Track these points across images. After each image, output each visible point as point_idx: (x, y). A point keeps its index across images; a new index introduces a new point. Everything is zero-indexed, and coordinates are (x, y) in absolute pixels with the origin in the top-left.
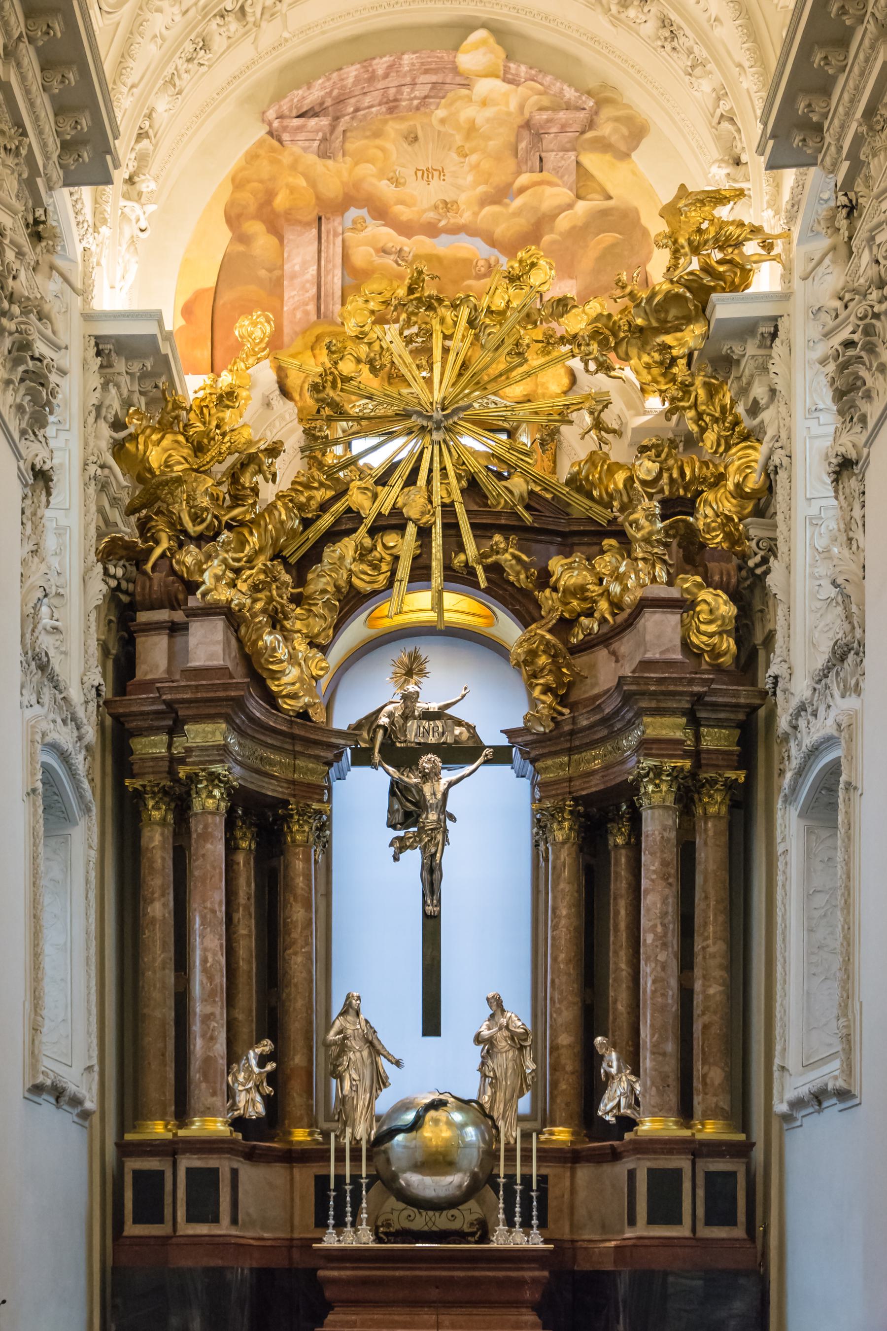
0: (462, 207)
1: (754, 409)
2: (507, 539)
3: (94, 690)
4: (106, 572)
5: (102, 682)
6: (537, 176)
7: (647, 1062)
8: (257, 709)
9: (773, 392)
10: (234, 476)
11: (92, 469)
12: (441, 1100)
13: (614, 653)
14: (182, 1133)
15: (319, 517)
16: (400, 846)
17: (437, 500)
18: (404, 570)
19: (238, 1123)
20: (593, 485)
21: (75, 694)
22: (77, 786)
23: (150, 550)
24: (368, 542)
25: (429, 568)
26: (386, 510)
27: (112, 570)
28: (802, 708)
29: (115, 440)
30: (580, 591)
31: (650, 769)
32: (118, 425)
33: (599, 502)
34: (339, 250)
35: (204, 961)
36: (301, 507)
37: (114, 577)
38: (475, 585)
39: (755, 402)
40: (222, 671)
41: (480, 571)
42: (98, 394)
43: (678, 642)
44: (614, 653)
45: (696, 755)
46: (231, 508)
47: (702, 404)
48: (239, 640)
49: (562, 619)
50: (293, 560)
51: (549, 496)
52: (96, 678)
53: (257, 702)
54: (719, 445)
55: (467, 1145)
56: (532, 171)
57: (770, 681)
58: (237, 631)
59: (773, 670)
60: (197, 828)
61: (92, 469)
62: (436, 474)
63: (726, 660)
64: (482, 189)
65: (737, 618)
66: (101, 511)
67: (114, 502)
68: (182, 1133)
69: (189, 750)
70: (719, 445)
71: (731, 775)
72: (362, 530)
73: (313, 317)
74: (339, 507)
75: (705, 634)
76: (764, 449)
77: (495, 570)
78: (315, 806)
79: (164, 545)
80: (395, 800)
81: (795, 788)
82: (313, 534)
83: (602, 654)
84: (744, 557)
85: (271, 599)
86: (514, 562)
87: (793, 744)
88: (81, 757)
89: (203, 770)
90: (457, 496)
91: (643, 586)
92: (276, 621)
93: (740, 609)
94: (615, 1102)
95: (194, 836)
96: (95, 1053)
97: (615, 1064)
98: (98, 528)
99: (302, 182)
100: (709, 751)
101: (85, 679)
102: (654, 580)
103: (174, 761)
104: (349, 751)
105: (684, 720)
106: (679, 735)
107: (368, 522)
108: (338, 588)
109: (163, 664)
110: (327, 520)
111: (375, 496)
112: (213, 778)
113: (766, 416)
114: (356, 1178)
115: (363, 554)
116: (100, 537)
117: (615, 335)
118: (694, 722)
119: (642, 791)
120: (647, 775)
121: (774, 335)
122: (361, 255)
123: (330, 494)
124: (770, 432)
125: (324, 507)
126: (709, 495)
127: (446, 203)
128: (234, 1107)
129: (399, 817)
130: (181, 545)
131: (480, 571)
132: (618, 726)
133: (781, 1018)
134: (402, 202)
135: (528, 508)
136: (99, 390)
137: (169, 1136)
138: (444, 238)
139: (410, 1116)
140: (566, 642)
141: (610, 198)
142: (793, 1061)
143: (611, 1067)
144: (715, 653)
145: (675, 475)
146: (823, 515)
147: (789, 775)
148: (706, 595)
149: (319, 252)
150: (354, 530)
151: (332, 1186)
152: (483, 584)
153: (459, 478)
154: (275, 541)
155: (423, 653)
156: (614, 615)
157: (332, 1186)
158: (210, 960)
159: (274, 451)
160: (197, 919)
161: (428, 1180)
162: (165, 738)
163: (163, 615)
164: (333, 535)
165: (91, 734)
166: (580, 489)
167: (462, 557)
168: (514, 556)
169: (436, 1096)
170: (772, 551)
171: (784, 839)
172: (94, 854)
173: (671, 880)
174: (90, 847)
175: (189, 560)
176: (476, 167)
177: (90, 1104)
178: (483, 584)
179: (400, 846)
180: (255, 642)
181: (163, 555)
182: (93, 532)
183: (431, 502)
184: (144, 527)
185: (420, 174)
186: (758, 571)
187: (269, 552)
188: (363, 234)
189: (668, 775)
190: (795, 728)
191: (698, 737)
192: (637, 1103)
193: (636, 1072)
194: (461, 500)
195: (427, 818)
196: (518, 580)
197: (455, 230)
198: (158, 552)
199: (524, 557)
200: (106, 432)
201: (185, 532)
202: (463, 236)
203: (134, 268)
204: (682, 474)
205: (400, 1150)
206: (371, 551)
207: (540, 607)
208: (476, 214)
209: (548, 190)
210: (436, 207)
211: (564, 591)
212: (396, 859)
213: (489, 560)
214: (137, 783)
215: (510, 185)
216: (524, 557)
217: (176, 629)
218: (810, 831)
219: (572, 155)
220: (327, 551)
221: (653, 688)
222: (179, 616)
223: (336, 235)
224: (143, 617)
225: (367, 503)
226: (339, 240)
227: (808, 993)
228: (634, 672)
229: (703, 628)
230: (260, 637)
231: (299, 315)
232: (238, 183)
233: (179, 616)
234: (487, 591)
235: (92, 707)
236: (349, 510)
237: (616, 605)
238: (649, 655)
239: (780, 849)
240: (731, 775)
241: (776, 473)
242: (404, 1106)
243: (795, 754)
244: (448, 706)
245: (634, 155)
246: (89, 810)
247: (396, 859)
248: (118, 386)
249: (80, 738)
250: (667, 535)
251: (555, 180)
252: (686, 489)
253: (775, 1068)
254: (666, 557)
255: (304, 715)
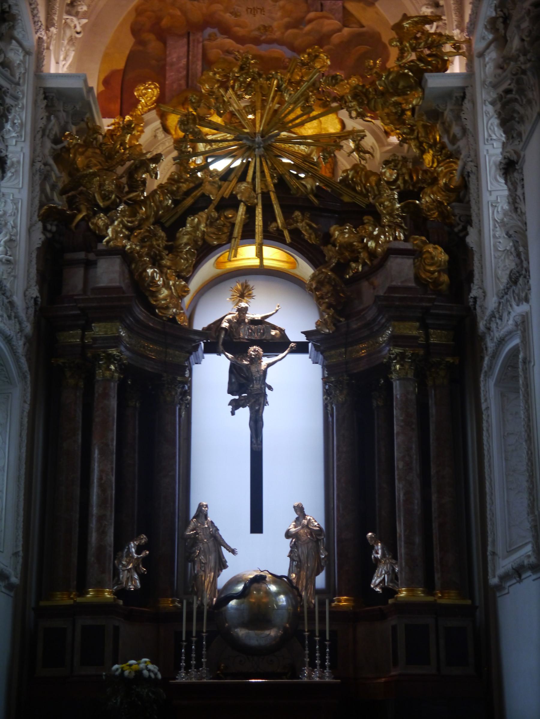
0: (276, 29)
1: (454, 140)
2: (303, 214)
3: (33, 300)
4: (45, 229)
5: (38, 295)
6: (319, 14)
7: (402, 550)
8: (140, 313)
9: (464, 131)
10: (131, 173)
11: (38, 165)
12: (261, 576)
13: (372, 284)
14: (79, 600)
15: (184, 199)
16: (235, 405)
17: (259, 190)
18: (237, 231)
19: (122, 593)
20: (355, 183)
21: (18, 300)
22: (17, 361)
23: (74, 216)
24: (215, 214)
25: (254, 231)
26: (227, 194)
27: (49, 227)
28: (493, 316)
29: (54, 149)
30: (349, 246)
31: (397, 355)
32: (56, 141)
33: (360, 193)
34: (200, 51)
35: (100, 479)
36: (172, 193)
37: (50, 231)
38: (283, 241)
39: (454, 136)
40: (118, 289)
41: (286, 233)
42: (44, 121)
43: (412, 275)
44: (372, 284)
45: (427, 346)
46: (128, 193)
47: (422, 137)
48: (131, 273)
49: (338, 264)
50: (167, 225)
51: (329, 190)
52: (35, 292)
53: (141, 310)
54: (433, 163)
55: (280, 608)
56: (316, 11)
57: (471, 300)
58: (129, 266)
59: (473, 293)
60: (99, 389)
61: (38, 165)
62: (258, 174)
63: (444, 287)
64: (286, 20)
65: (449, 262)
66: (43, 190)
67: (53, 187)
68: (79, 600)
69: (95, 339)
70: (433, 163)
71: (449, 359)
72: (212, 207)
73: (184, 87)
74: (197, 193)
75: (429, 271)
76: (460, 163)
77: (296, 233)
78: (179, 379)
79: (84, 214)
80: (233, 376)
81: (491, 367)
82: (181, 209)
83: (365, 285)
84: (451, 226)
85: (151, 247)
86: (308, 228)
87: (488, 340)
88: (21, 343)
89: (104, 352)
90: (271, 187)
91: (389, 241)
92: (156, 262)
93: (450, 257)
94: (381, 578)
95: (96, 395)
96: (20, 543)
97: (380, 552)
98: (41, 202)
99: (179, 13)
100: (435, 344)
101: (27, 293)
102: (395, 238)
103: (84, 347)
104: (202, 344)
105: (418, 324)
106: (415, 333)
107: (215, 203)
108: (196, 242)
109: (80, 286)
110: (189, 201)
111: (220, 187)
112: (110, 359)
113: (461, 144)
114: (199, 632)
115: (211, 223)
116: (41, 206)
117: (367, 97)
118: (425, 327)
119: (393, 368)
120: (395, 358)
121: (464, 97)
122: (214, 53)
123: (192, 185)
124: (464, 153)
125: (188, 193)
126: (428, 190)
127: (264, 27)
128: (118, 582)
129: (235, 387)
130: (95, 214)
131: (286, 233)
132: (376, 328)
133: (491, 520)
134: (239, 26)
135: (316, 196)
136: (45, 119)
137: (71, 602)
138: (264, 46)
139: (240, 587)
140: (342, 277)
141: (363, 26)
142: (500, 549)
143: (378, 553)
144: (436, 282)
145: (407, 178)
146: (499, 200)
147: (486, 359)
148: (430, 248)
149: (188, 51)
150: (206, 208)
151: (184, 638)
152: (288, 240)
153: (272, 177)
154: (156, 213)
155: (251, 284)
156: (371, 260)
157: (184, 638)
158: (104, 478)
159: (157, 159)
160: (97, 452)
161: (252, 633)
162: (79, 331)
163: (82, 255)
164: (193, 210)
165: (28, 328)
166: (348, 186)
167: (274, 225)
168: (308, 225)
169: (258, 573)
170: (469, 222)
171: (486, 400)
172: (27, 407)
173: (414, 426)
174: (25, 402)
175: (101, 223)
176: (282, 8)
177: (14, 580)
178: (288, 240)
179: (235, 405)
180: (141, 273)
181: (83, 219)
182: (37, 202)
183: (254, 190)
184: (71, 202)
185: (249, 10)
186: (461, 235)
187: (152, 220)
188: (215, 43)
189: (409, 359)
190: (489, 329)
191: (427, 336)
192: (397, 578)
193: (395, 557)
194: (273, 189)
195: (253, 387)
196: (310, 238)
197: (270, 42)
198: (80, 216)
199: (314, 225)
200: (49, 144)
201: (98, 206)
202: (275, 45)
203: (72, 54)
204: (411, 177)
205: (232, 608)
206: (217, 219)
207: (324, 256)
208: (283, 33)
209: (327, 22)
210: (259, 29)
211: (340, 246)
212: (233, 413)
213: (292, 227)
214: (61, 361)
215: (304, 18)
216: (314, 225)
217: (90, 265)
218: (502, 395)
219: (340, 3)
220: (189, 219)
221: (397, 303)
222: (92, 256)
223: (199, 42)
224: (69, 256)
225: (214, 191)
226: (200, 45)
227: (508, 502)
228: (385, 293)
229: (428, 268)
230: (145, 270)
231: (175, 86)
232: (139, 11)
233: (92, 256)
234: (291, 245)
235: (31, 311)
236: (203, 195)
237: (372, 254)
238: (394, 283)
239: (484, 406)
240: (449, 359)
241: (469, 176)
242: (235, 581)
243: (491, 345)
244: (267, 317)
245: (377, 4)
246: (25, 377)
247: (233, 413)
248: (57, 117)
249: (21, 330)
250: (403, 212)
251: (331, 16)
252: (414, 185)
253: (488, 553)
254: (403, 225)
255: (173, 320)
